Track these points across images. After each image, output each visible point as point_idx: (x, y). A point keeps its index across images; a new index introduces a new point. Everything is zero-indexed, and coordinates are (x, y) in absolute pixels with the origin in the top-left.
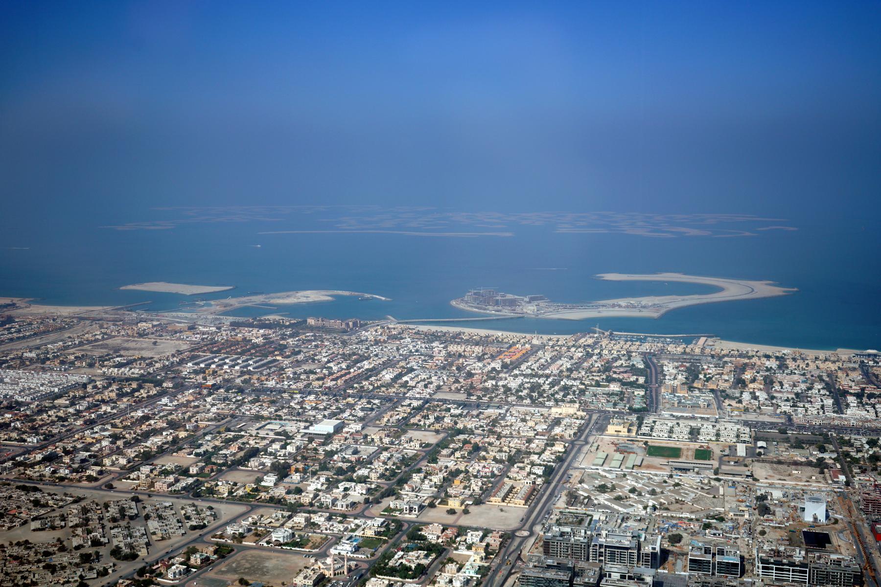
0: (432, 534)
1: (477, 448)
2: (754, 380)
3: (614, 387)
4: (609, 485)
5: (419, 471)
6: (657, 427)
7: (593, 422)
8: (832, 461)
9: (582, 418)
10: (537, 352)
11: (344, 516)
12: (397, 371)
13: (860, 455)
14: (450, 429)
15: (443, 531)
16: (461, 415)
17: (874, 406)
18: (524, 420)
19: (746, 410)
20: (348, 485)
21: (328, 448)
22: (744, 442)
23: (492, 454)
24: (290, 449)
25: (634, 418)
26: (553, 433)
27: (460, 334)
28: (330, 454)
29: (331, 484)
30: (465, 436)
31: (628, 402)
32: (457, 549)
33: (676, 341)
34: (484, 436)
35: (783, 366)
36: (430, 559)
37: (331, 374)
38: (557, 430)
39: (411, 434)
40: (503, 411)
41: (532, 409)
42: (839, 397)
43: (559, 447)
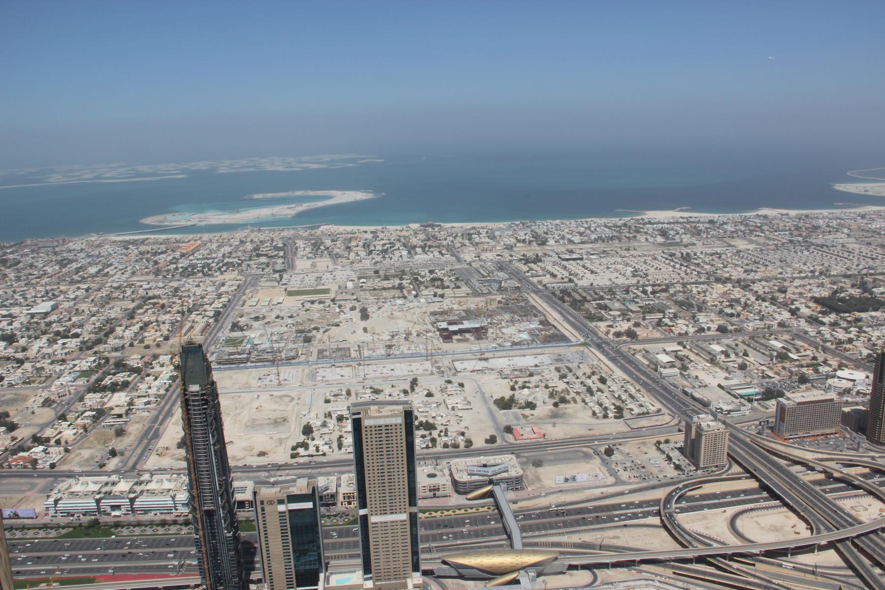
0: (134, 360)
1: (163, 306)
2: (357, 246)
3: (263, 260)
4: (261, 316)
5: (121, 325)
6: (293, 279)
7: (248, 282)
8: (407, 285)
9: (240, 280)
10: (206, 245)
11: (63, 361)
12: (100, 267)
13: (424, 279)
14: (143, 297)
15: (141, 359)
16: (150, 289)
17: (432, 252)
18: (198, 286)
19: (352, 263)
20: (64, 341)
21: (47, 320)
22: (352, 281)
23: (175, 309)
24: (16, 324)
25: (277, 275)
26: (220, 291)
27: (147, 239)
28: (49, 324)
29: (51, 342)
30: (155, 300)
31: (273, 267)
32: (153, 368)
33: (306, 229)
34: (169, 299)
35: (376, 237)
36: (133, 377)
37: (45, 274)
38: (223, 289)
39: (112, 303)
40: (182, 283)
41: (203, 279)
42: (411, 249)
43: (224, 299)
